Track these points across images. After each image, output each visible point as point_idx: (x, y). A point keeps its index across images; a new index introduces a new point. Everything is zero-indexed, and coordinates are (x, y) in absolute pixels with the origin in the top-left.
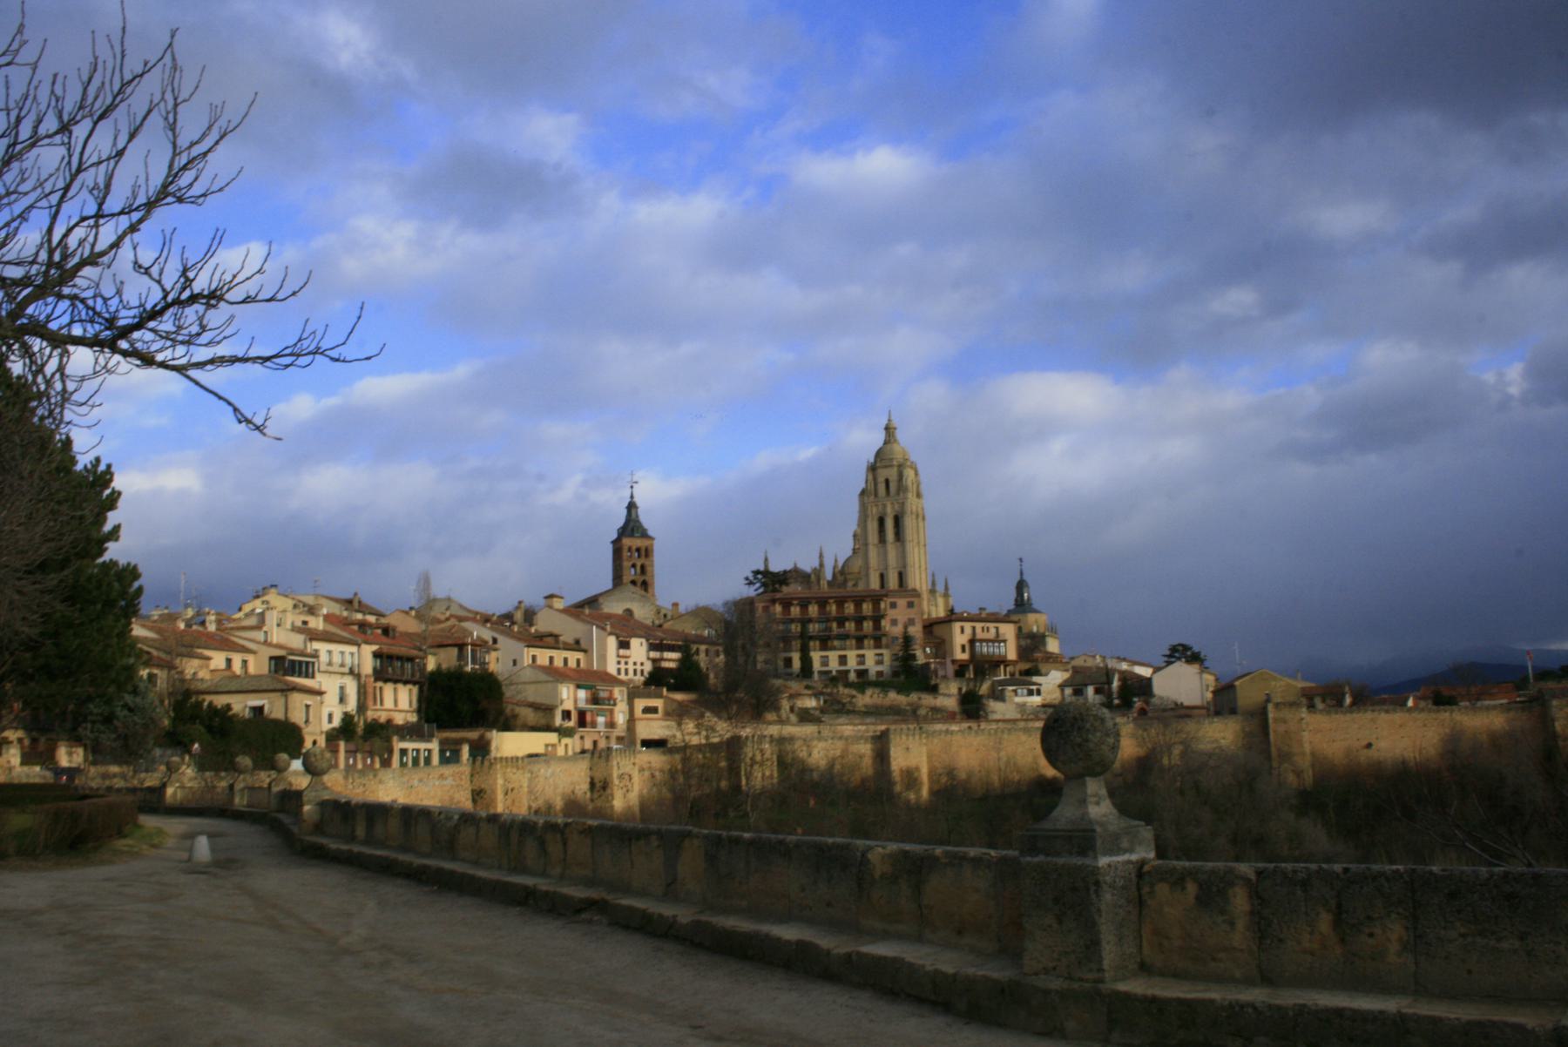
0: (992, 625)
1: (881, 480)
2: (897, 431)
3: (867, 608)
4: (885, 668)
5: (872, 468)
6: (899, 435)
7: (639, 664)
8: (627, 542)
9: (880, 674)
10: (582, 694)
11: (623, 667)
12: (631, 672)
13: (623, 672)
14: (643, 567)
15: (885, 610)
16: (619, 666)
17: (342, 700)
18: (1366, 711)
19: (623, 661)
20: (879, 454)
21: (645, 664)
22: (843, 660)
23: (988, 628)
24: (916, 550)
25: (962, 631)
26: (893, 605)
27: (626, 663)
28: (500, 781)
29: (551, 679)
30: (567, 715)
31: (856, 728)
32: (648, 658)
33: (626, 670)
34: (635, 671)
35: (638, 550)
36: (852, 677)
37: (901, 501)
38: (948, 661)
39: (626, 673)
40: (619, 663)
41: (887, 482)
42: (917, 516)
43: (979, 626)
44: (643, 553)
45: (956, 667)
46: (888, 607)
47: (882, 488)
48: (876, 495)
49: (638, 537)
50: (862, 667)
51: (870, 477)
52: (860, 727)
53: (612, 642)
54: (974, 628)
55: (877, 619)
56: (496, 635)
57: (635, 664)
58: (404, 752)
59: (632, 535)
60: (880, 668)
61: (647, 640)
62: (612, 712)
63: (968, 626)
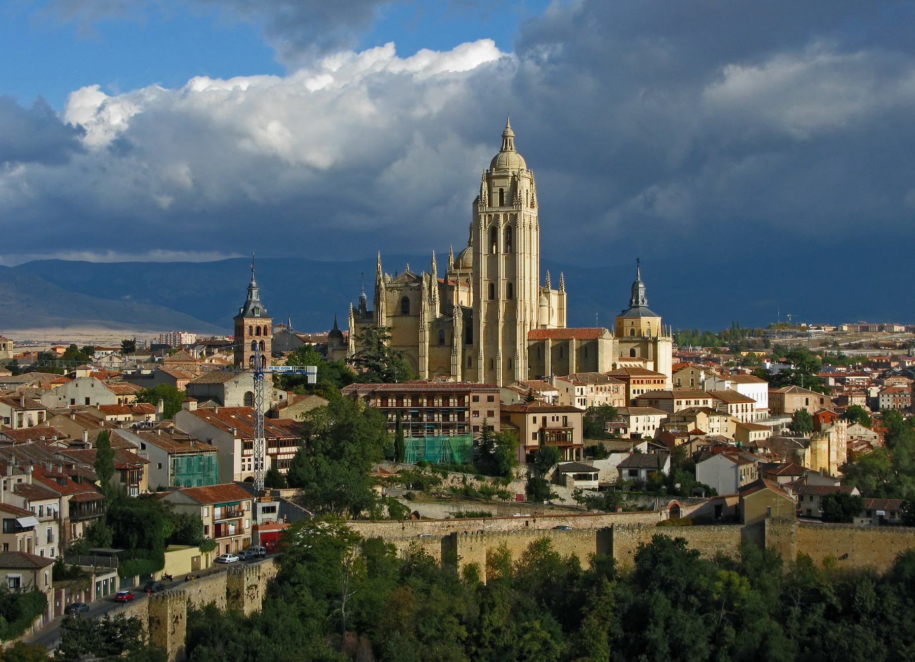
0: (560, 415)
1: (496, 190)
8: (248, 322)
10: (218, 511)
11: (246, 463)
15: (469, 402)
16: (243, 463)
17: (50, 540)
18: (845, 528)
19: (246, 459)
23: (557, 417)
24: (527, 261)
25: (535, 419)
26: (476, 399)
27: (249, 460)
28: (169, 611)
35: (258, 328)
37: (514, 213)
40: (243, 460)
41: (501, 191)
43: (549, 416)
46: (471, 400)
49: (258, 317)
51: (485, 185)
53: (238, 443)
54: (544, 419)
56: (145, 443)
58: (98, 584)
59: (252, 316)
61: (267, 439)
62: (240, 521)
63: (539, 417)
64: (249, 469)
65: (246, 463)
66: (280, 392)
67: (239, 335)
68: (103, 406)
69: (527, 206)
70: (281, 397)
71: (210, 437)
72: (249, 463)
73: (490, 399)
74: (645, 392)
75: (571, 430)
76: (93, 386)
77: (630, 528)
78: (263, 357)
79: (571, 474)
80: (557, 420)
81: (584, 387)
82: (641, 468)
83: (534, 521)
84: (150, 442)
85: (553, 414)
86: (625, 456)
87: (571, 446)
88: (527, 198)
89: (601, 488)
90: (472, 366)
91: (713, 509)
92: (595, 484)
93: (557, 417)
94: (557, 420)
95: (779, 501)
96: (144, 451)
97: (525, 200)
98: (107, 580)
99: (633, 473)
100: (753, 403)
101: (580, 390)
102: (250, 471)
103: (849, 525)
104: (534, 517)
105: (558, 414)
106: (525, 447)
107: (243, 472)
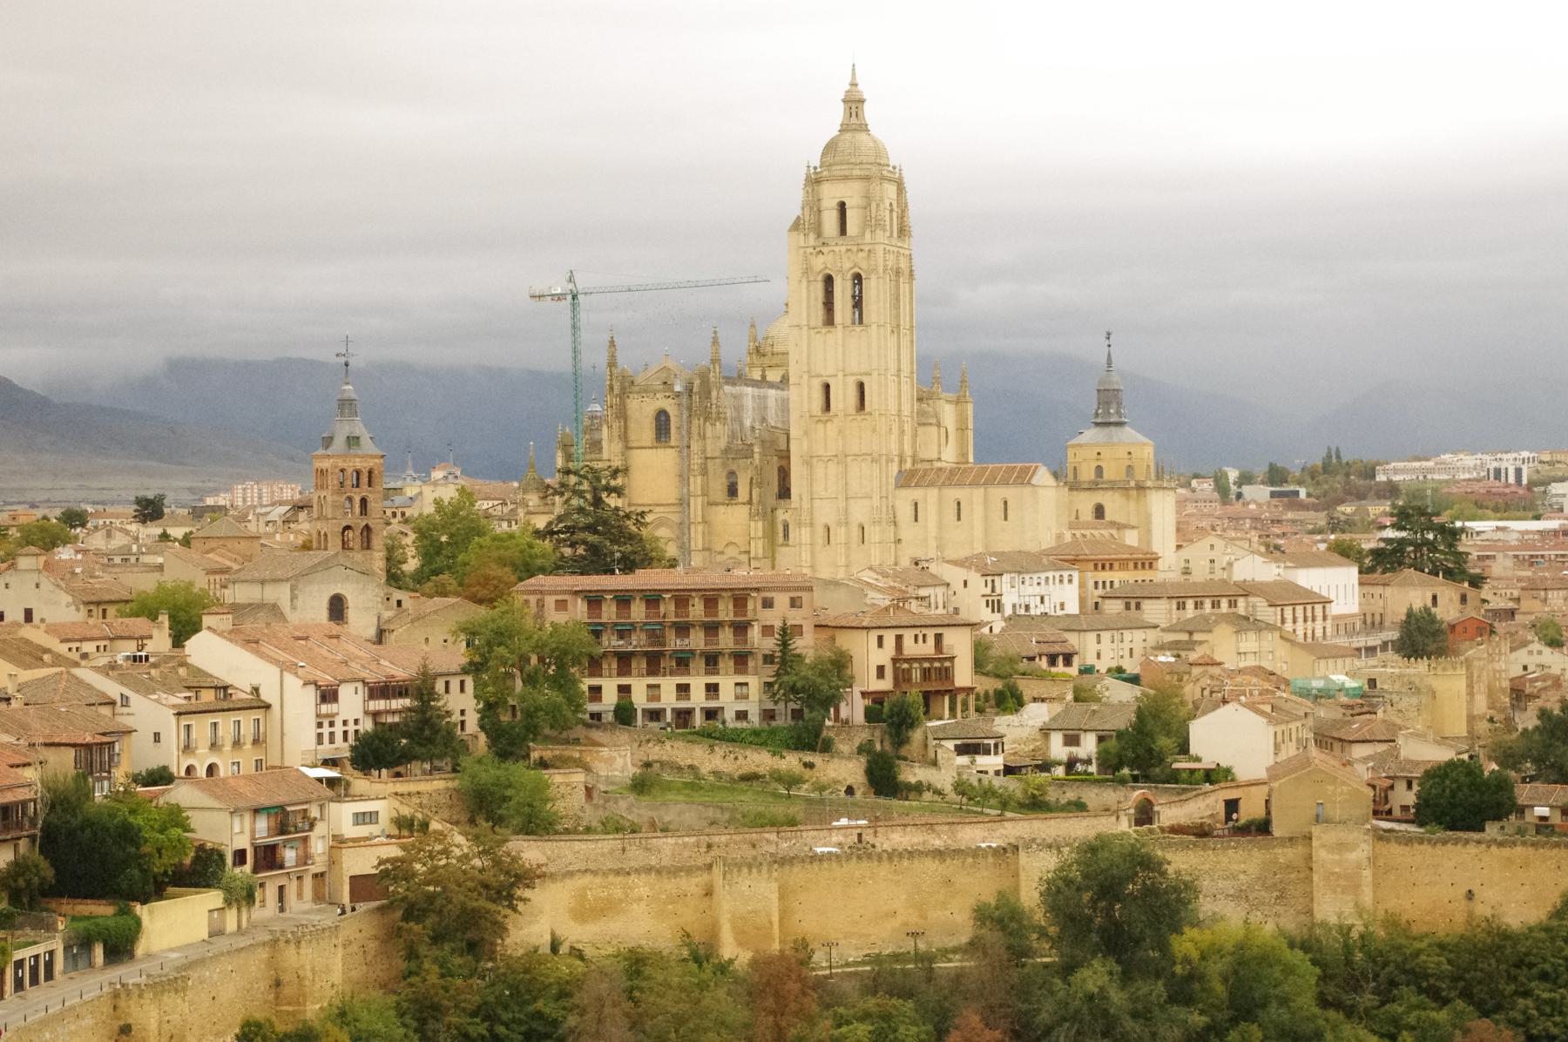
0: (931, 633)
2: (866, 106)
3: (726, 612)
4: (753, 708)
5: (814, 181)
6: (870, 113)
7: (351, 723)
9: (742, 715)
10: (262, 824)
11: (326, 730)
12: (339, 737)
13: (326, 738)
14: (364, 501)
16: (320, 731)
18: (1467, 842)
20: (831, 147)
21: (361, 722)
22: (683, 689)
23: (924, 636)
25: (880, 638)
26: (768, 604)
27: (332, 724)
29: (216, 804)
30: (240, 856)
31: (680, 841)
32: (366, 713)
33: (332, 734)
34: (345, 733)
36: (698, 720)
38: (857, 690)
39: (332, 741)
40: (320, 725)
41: (842, 207)
42: (898, 273)
44: (364, 479)
45: (868, 702)
47: (830, 220)
48: (819, 235)
50: (713, 704)
52: (686, 839)
53: (311, 694)
54: (899, 638)
55: (741, 628)
56: (127, 692)
57: (345, 723)
58: (19, 964)
60: (742, 707)
62: (305, 839)
64: (332, 741)
65: (326, 730)
66: (397, 595)
67: (322, 487)
68: (55, 625)
69: (891, 236)
70: (399, 603)
71: (255, 683)
72: (332, 729)
73: (794, 603)
74: (1116, 585)
75: (952, 659)
76: (37, 586)
77: (1054, 846)
78: (367, 527)
79: (950, 745)
80: (924, 641)
81: (996, 578)
82: (1085, 731)
83: (876, 832)
84: (138, 692)
85: (917, 631)
86: (1057, 708)
87: (950, 691)
88: (891, 220)
89: (1009, 770)
90: (791, 542)
91: (1221, 809)
92: (993, 762)
93: (924, 636)
94: (924, 641)
95: (1339, 790)
96: (125, 710)
97: (888, 223)
98: (37, 957)
99: (1072, 740)
100: (1327, 605)
101: (990, 584)
102: (332, 746)
103: (1476, 836)
104: (875, 822)
105: (925, 631)
106: (864, 694)
107: (320, 747)
